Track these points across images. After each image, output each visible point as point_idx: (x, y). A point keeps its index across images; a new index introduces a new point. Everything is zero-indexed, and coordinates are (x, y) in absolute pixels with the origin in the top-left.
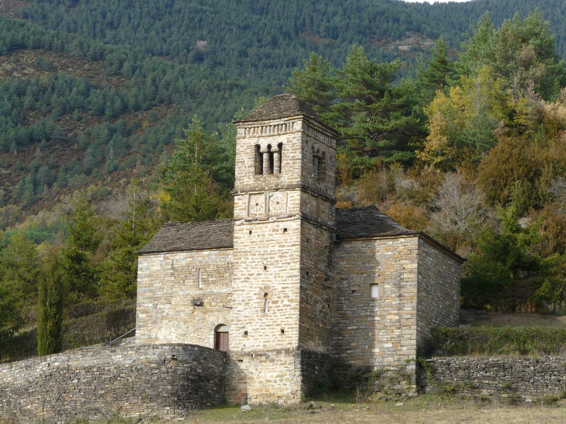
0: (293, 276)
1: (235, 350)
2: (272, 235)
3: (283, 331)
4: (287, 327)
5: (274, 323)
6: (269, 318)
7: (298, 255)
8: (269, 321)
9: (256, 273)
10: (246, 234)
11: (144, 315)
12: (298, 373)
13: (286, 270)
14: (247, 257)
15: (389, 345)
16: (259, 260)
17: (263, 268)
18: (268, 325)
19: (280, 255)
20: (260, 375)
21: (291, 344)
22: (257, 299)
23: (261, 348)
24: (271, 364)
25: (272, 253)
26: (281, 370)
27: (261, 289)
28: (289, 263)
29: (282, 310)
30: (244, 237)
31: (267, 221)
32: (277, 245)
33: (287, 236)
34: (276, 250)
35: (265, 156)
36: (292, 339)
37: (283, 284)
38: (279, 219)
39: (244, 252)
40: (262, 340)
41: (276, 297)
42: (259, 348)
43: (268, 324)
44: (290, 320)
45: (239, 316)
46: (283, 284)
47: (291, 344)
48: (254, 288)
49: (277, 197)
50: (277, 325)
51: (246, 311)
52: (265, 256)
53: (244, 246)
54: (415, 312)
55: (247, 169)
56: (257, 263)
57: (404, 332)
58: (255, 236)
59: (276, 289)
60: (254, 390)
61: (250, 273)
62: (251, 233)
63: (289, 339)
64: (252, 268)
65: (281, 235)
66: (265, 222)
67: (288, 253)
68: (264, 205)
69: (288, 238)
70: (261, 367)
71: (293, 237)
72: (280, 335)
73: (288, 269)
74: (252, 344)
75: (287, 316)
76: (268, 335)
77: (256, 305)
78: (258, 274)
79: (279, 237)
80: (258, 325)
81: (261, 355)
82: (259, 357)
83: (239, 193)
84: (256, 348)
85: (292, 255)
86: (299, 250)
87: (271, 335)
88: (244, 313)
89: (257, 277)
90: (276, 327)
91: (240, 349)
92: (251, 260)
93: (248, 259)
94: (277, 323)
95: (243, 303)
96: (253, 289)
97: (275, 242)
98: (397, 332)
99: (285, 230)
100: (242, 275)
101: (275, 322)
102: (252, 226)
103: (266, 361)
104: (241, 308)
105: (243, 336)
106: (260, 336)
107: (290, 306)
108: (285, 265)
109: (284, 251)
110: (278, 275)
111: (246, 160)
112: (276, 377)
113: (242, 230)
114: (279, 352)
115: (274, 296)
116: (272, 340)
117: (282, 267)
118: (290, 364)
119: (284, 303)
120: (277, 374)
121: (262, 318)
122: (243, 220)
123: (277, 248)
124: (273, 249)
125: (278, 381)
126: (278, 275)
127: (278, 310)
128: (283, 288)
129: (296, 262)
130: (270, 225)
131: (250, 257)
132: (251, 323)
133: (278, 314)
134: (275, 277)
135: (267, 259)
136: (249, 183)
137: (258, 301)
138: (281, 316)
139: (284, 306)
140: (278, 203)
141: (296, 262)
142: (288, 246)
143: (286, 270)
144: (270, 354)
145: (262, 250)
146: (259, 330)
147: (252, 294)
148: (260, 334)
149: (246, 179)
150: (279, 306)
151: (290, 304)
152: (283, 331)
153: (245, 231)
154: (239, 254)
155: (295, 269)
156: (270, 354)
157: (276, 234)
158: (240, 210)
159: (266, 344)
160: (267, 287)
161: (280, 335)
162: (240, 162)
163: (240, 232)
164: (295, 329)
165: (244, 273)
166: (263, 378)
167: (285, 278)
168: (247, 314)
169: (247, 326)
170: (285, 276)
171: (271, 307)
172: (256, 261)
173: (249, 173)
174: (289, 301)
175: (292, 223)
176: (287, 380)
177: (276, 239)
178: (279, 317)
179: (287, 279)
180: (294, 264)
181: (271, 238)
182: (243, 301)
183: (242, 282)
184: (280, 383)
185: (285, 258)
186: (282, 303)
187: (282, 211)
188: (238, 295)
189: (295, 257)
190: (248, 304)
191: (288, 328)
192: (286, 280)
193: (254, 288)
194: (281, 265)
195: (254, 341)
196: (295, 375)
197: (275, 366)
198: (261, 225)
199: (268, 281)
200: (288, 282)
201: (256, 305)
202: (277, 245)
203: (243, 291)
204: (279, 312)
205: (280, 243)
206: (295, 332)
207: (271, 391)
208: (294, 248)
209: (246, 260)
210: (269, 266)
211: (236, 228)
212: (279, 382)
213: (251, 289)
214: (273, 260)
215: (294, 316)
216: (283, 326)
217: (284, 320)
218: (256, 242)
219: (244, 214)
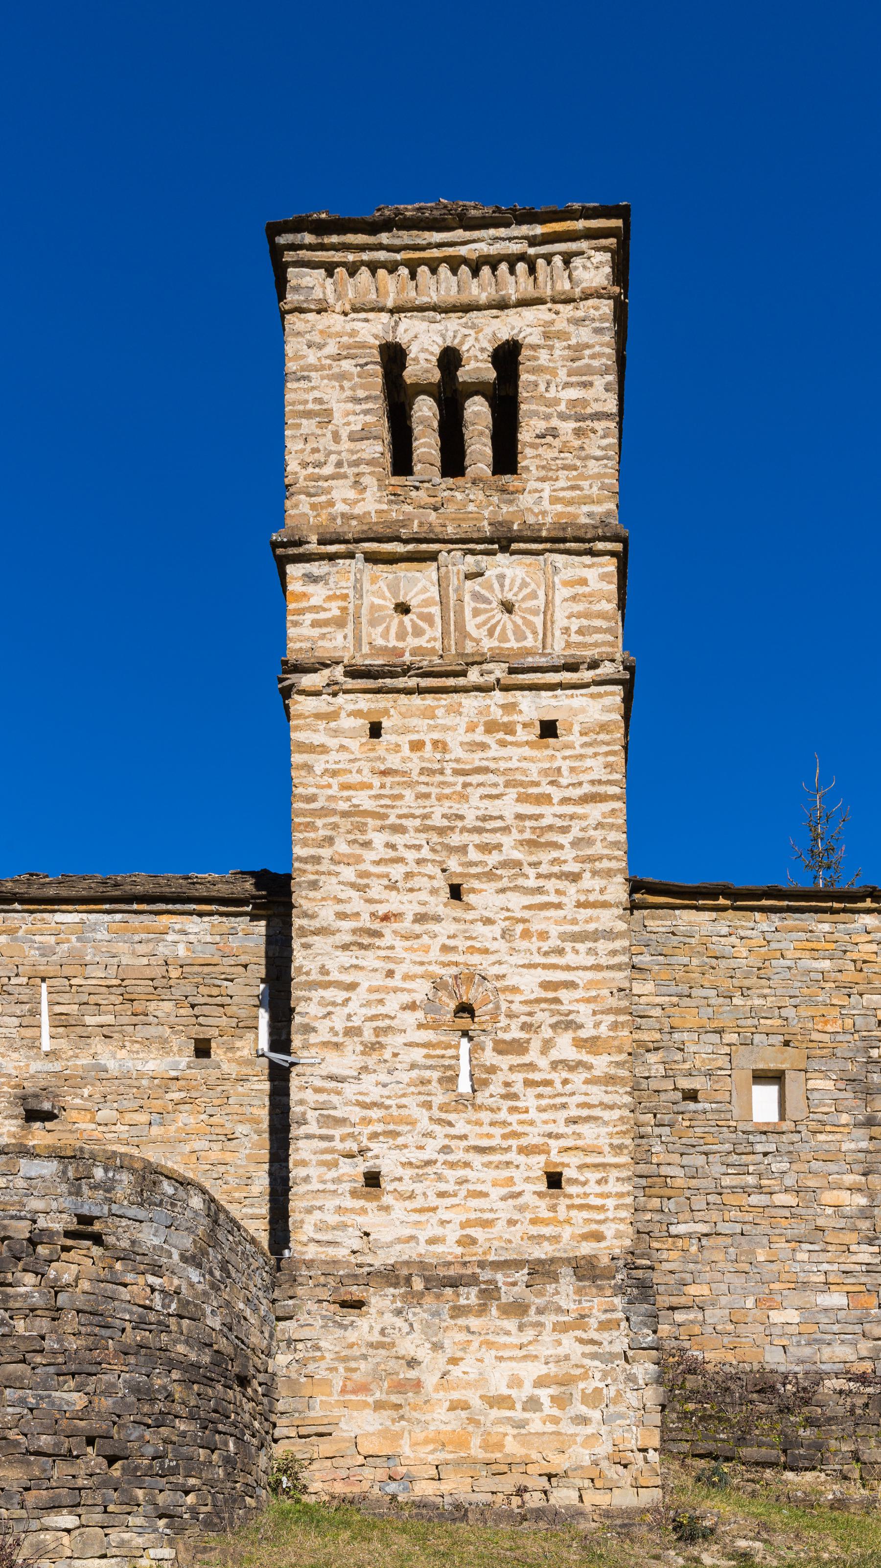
0: (595, 936)
1: (311, 1252)
2: (483, 746)
3: (554, 1180)
5: (514, 1143)
7: (615, 844)
8: (486, 1129)
9: (410, 910)
10: (352, 734)
14: (361, 838)
16: (425, 853)
17: (446, 892)
19: (527, 835)
20: (456, 1371)
21: (598, 1237)
22: (420, 1026)
23: (450, 1249)
24: (511, 1324)
25: (490, 825)
26: (561, 1351)
27: (438, 985)
28: (575, 877)
29: (548, 1083)
30: (342, 747)
31: (461, 681)
32: (513, 793)
35: (425, 410)
37: (545, 967)
38: (522, 675)
39: (345, 814)
41: (515, 1024)
43: (485, 1143)
45: (335, 1099)
46: (545, 967)
47: (598, 1237)
48: (406, 977)
49: (501, 577)
52: (455, 839)
53: (345, 787)
55: (345, 445)
56: (413, 867)
58: (397, 748)
59: (515, 990)
60: (427, 1441)
61: (382, 909)
63: (585, 1214)
64: (393, 887)
65: (526, 751)
66: (451, 682)
67: (565, 830)
68: (435, 610)
69: (565, 765)
70: (463, 1336)
71: (589, 763)
72: (540, 1194)
73: (569, 901)
74: (407, 1232)
75: (574, 1112)
76: (484, 1195)
77: (418, 1055)
78: (421, 918)
79: (524, 757)
81: (454, 1283)
82: (449, 1291)
83: (313, 547)
84: (422, 1248)
85: (590, 842)
86: (621, 821)
87: (496, 1193)
88: (362, 1088)
89: (418, 928)
90: (521, 1159)
91: (341, 1253)
92: (379, 851)
93: (367, 844)
94: (524, 1141)
96: (397, 982)
97: (501, 780)
99: (549, 729)
100: (342, 916)
102: (383, 701)
103: (482, 1310)
104: (344, 1062)
105: (354, 1194)
106: (441, 1195)
107: (589, 1067)
108: (551, 885)
109: (544, 822)
110: (520, 928)
111: (339, 409)
112: (540, 1383)
113: (332, 716)
114: (541, 1271)
115: (503, 1021)
116: (504, 1216)
117: (539, 890)
118: (604, 1326)
119: (555, 1054)
120: (537, 1369)
121: (451, 1117)
122: (340, 669)
124: (492, 808)
125: (546, 1401)
126: (520, 928)
127: (528, 1083)
128: (546, 985)
129: (609, 873)
130: (471, 703)
132: (395, 1134)
133: (529, 1099)
135: (463, 849)
136: (358, 510)
139: (555, 1065)
140: (508, 607)
141: (609, 873)
142: (565, 801)
143: (559, 906)
144: (500, 1277)
145: (438, 812)
146: (438, 1168)
147: (392, 1004)
148: (443, 1187)
149: (342, 494)
150: (531, 1066)
152: (554, 1180)
153: (346, 722)
154: (319, 823)
155: (605, 905)
156: (500, 1277)
157: (503, 744)
158: (315, 624)
160: (469, 978)
162: (308, 414)
163: (322, 725)
164: (614, 1174)
165: (348, 908)
166: (468, 1385)
167: (554, 942)
168: (375, 1094)
169: (376, 1147)
170: (554, 931)
171: (492, 1069)
172: (411, 856)
173: (356, 463)
174: (579, 1043)
175: (577, 700)
176: (593, 1398)
177: (503, 765)
178: (533, 1114)
179: (568, 946)
180: (597, 883)
181: (476, 759)
182: (352, 1032)
183: (345, 947)
184: (556, 1412)
185: (555, 854)
186: (544, 1051)
187: (529, 643)
188: (323, 1003)
189: (598, 849)
190: (374, 1047)
191: (580, 1167)
192: (560, 952)
193: (406, 977)
194: (532, 883)
195: (416, 1217)
196: (631, 1378)
197: (529, 1334)
198: (429, 700)
199: (472, 950)
200: (570, 958)
201: (418, 1055)
202: (513, 793)
204: (531, 1092)
205: (522, 784)
206: (613, 1187)
207: (512, 1447)
208: (595, 812)
209: (357, 850)
210: (476, 884)
211: (300, 705)
212: (548, 1409)
213: (390, 983)
214: (493, 858)
215: (607, 1115)
216: (555, 1157)
217: (562, 1129)
218: (404, 773)
219: (338, 643)
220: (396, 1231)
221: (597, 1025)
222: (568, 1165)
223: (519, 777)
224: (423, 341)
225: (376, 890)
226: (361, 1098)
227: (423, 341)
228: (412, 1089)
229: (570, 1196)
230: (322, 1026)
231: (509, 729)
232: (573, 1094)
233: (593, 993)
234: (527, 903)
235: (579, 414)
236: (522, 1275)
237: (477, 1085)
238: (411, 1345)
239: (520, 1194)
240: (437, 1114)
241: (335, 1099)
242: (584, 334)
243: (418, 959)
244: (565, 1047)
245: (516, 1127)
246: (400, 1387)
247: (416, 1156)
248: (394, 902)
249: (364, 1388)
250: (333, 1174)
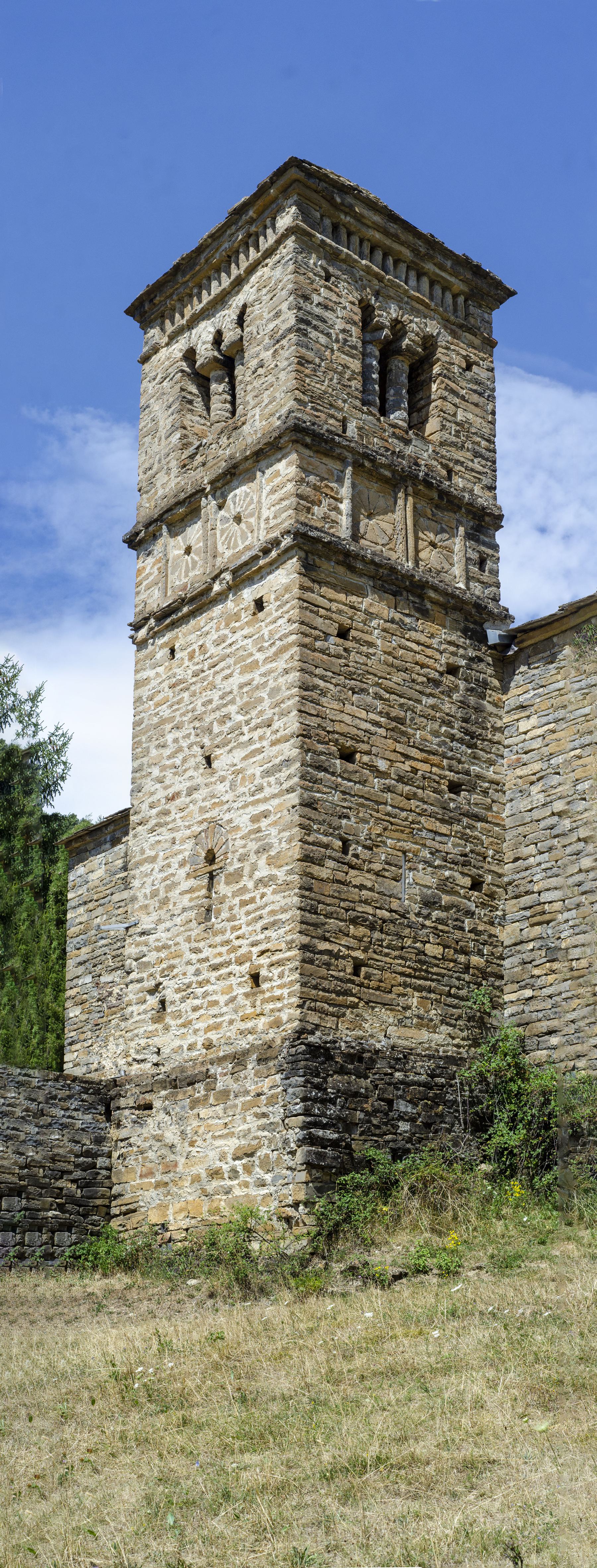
4: (264, 961)
6: (218, 939)
13: (260, 751)
18: (215, 968)
34: (235, 688)
37: (254, 803)
40: (201, 1025)
42: (195, 1053)
47: (277, 1024)
51: (161, 927)
61: (171, 792)
62: (173, 651)
76: (216, 1003)
77: (185, 901)
78: (191, 791)
80: (191, 969)
84: (186, 1055)
87: (222, 999)
101: (234, 949)
106: (195, 1009)
108: (256, 735)
114: (238, 1059)
119: (258, 875)
120: (231, 1145)
121: (201, 945)
124: (227, 686)
127: (244, 903)
128: (255, 819)
134: (233, 786)
137: (192, 882)
138: (248, 924)
143: (260, 751)
151: (275, 871)
161: (247, 995)
165: (154, 798)
170: (258, 771)
182: (154, 894)
183: (152, 830)
192: (260, 789)
194: (245, 738)
200: (268, 791)
203: (153, 859)
209: (161, 751)
210: (218, 752)
215: (284, 917)
221: (280, 843)
222: (262, 966)
223: (241, 653)
226: (157, 944)
228: (182, 929)
229: (263, 992)
230: (140, 895)
231: (237, 617)
232: (266, 905)
233: (279, 815)
234: (243, 755)
239: (235, 998)
240: (194, 945)
241: (145, 949)
243: (187, 824)
245: (237, 943)
249: (151, 1173)
250: (144, 1007)
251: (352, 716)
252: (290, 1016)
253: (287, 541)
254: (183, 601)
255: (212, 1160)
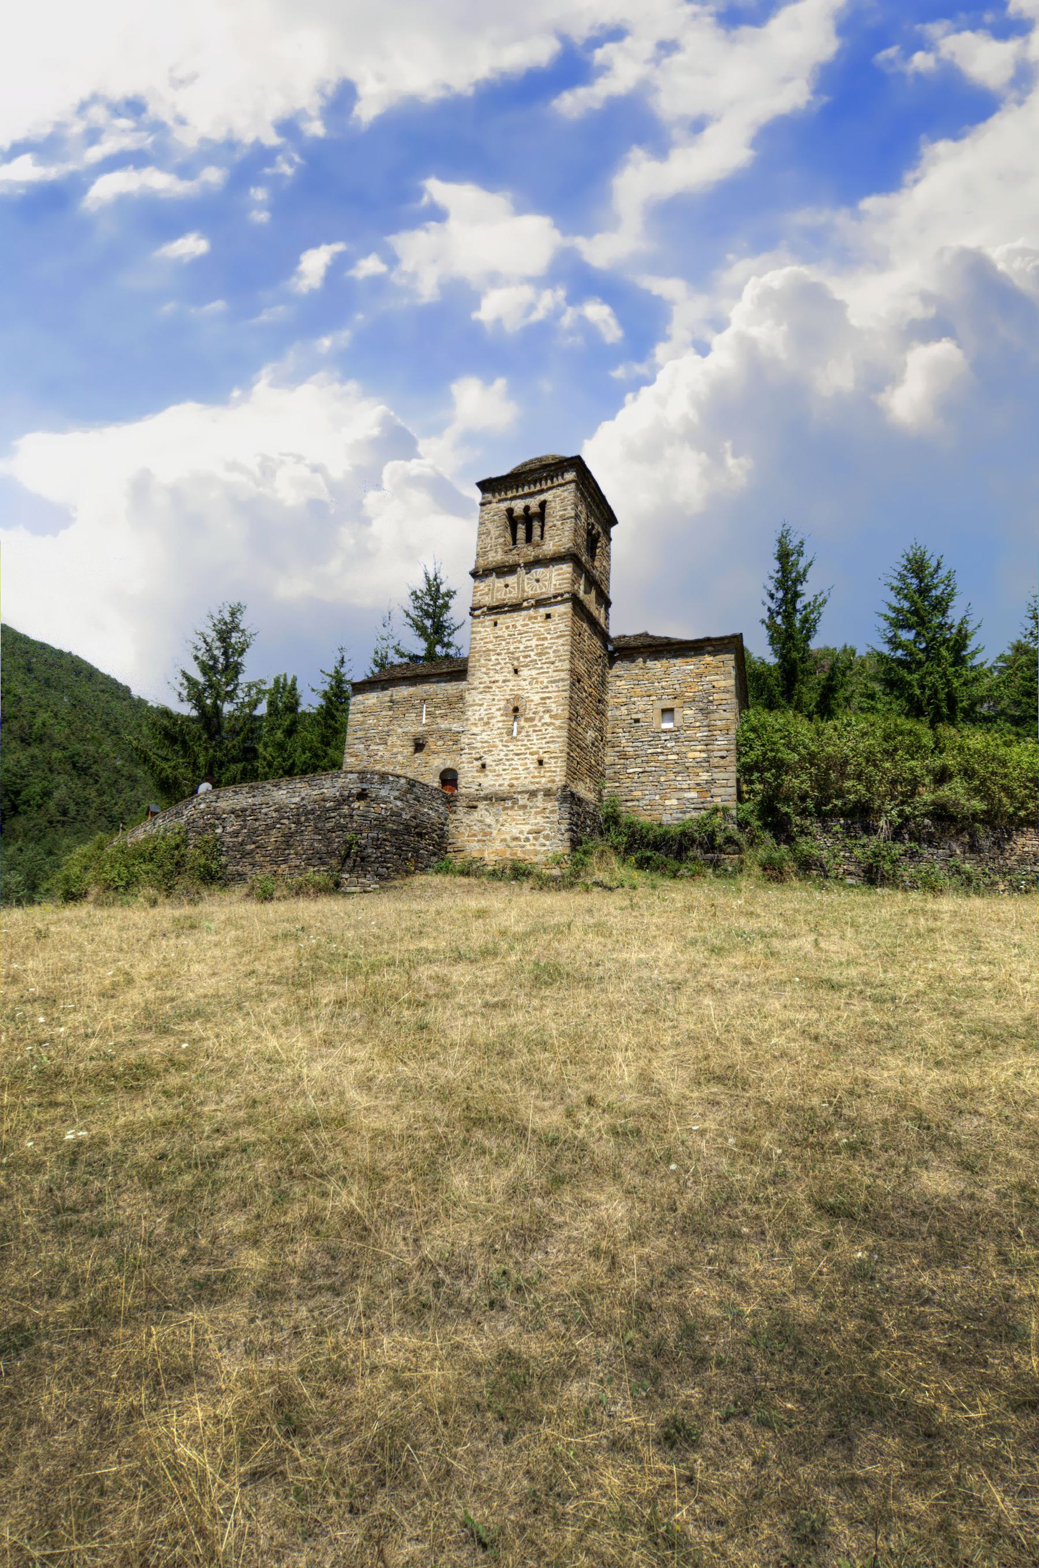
1: (463, 791)
3: (541, 762)
11: (353, 759)
12: (564, 827)
15: (693, 794)
23: (505, 788)
24: (521, 812)
33: (551, 625)
36: (556, 773)
44: (552, 745)
47: (553, 781)
50: (532, 754)
54: (733, 747)
57: (715, 776)
62: (496, 624)
77: (500, 725)
79: (539, 626)
95: (480, 723)
98: (705, 776)
99: (548, 616)
103: (512, 808)
114: (533, 794)
123: (534, 643)
124: (529, 644)
128: (542, 699)
131: (493, 658)
134: (530, 683)
140: (538, 581)
152: (541, 762)
159: (515, 782)
160: (518, 698)
168: (486, 738)
174: (551, 717)
182: (481, 719)
190: (488, 723)
201: (500, 725)
212: (532, 841)
220: (490, 782)
224: (518, 506)
225: (492, 673)
227: (518, 506)
235: (563, 518)
236: (526, 796)
237: (519, 733)
238: (489, 820)
242: (566, 494)
244: (547, 719)
246: (485, 834)
247: (496, 757)
248: (497, 677)
251: (581, 667)
252: (560, 779)
253: (566, 596)
254: (505, 605)
255: (515, 832)
